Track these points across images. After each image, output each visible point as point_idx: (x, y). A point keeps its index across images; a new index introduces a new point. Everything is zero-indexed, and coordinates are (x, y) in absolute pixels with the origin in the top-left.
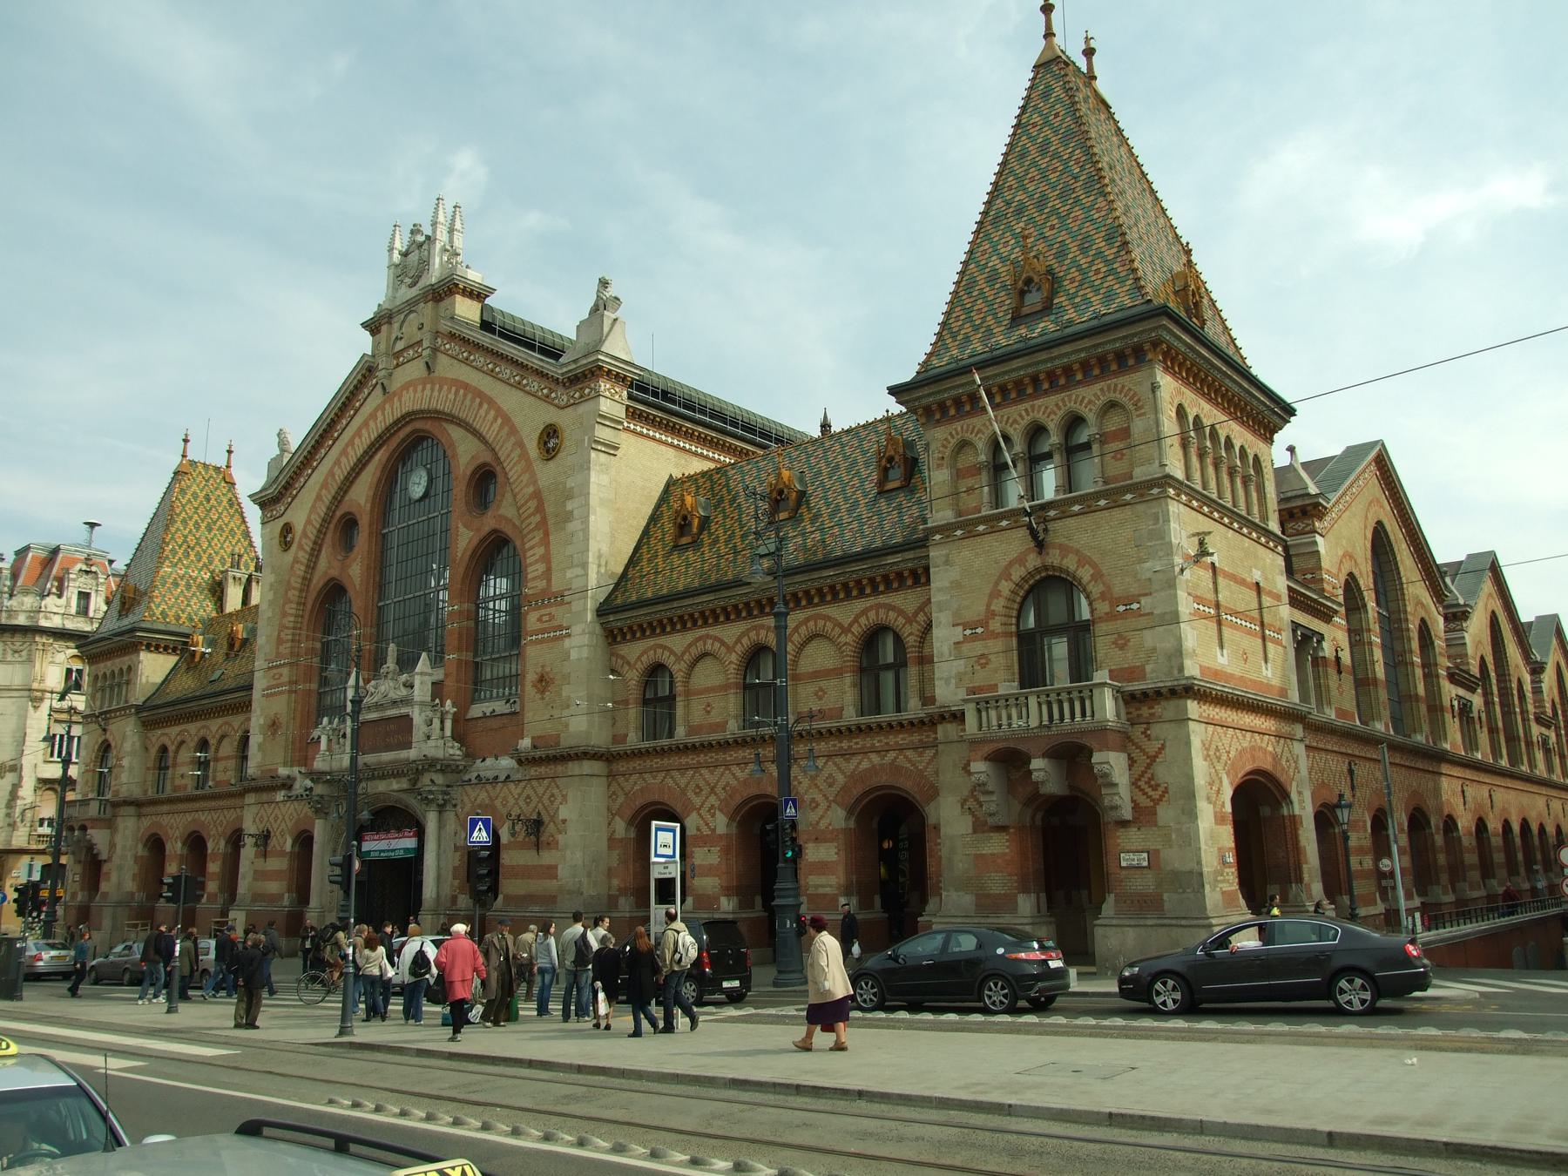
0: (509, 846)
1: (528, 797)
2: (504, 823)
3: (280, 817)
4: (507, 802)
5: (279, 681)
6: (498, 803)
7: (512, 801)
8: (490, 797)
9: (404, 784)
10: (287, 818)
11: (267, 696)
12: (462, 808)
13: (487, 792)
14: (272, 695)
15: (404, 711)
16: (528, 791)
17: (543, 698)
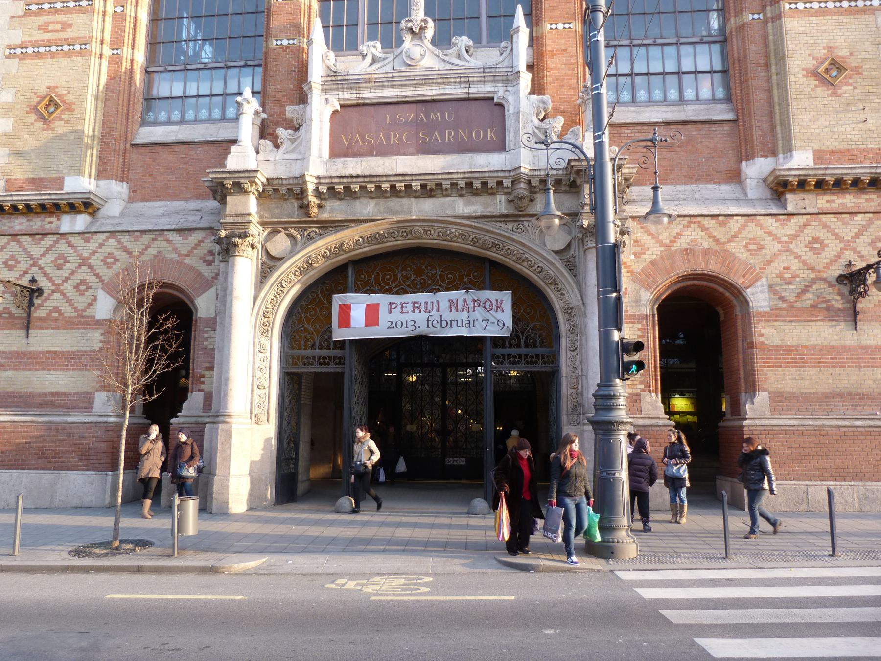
0: (773, 316)
1: (816, 240)
2: (757, 278)
3: (74, 260)
4: (761, 248)
5: (63, 35)
6: (737, 249)
7: (770, 246)
8: (716, 240)
9: (499, 204)
10: (95, 261)
11: (24, 57)
12: (637, 255)
13: (704, 229)
14: (37, 55)
15: (477, 89)
16: (814, 229)
17: (835, 94)
